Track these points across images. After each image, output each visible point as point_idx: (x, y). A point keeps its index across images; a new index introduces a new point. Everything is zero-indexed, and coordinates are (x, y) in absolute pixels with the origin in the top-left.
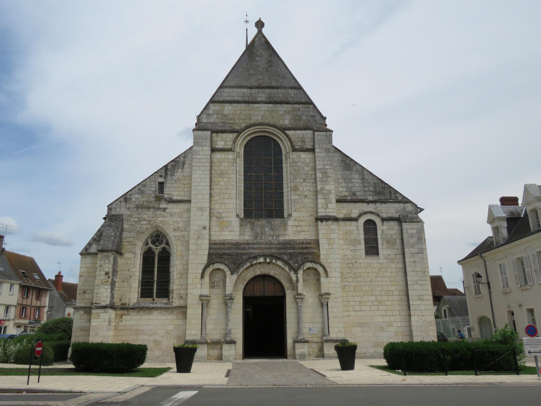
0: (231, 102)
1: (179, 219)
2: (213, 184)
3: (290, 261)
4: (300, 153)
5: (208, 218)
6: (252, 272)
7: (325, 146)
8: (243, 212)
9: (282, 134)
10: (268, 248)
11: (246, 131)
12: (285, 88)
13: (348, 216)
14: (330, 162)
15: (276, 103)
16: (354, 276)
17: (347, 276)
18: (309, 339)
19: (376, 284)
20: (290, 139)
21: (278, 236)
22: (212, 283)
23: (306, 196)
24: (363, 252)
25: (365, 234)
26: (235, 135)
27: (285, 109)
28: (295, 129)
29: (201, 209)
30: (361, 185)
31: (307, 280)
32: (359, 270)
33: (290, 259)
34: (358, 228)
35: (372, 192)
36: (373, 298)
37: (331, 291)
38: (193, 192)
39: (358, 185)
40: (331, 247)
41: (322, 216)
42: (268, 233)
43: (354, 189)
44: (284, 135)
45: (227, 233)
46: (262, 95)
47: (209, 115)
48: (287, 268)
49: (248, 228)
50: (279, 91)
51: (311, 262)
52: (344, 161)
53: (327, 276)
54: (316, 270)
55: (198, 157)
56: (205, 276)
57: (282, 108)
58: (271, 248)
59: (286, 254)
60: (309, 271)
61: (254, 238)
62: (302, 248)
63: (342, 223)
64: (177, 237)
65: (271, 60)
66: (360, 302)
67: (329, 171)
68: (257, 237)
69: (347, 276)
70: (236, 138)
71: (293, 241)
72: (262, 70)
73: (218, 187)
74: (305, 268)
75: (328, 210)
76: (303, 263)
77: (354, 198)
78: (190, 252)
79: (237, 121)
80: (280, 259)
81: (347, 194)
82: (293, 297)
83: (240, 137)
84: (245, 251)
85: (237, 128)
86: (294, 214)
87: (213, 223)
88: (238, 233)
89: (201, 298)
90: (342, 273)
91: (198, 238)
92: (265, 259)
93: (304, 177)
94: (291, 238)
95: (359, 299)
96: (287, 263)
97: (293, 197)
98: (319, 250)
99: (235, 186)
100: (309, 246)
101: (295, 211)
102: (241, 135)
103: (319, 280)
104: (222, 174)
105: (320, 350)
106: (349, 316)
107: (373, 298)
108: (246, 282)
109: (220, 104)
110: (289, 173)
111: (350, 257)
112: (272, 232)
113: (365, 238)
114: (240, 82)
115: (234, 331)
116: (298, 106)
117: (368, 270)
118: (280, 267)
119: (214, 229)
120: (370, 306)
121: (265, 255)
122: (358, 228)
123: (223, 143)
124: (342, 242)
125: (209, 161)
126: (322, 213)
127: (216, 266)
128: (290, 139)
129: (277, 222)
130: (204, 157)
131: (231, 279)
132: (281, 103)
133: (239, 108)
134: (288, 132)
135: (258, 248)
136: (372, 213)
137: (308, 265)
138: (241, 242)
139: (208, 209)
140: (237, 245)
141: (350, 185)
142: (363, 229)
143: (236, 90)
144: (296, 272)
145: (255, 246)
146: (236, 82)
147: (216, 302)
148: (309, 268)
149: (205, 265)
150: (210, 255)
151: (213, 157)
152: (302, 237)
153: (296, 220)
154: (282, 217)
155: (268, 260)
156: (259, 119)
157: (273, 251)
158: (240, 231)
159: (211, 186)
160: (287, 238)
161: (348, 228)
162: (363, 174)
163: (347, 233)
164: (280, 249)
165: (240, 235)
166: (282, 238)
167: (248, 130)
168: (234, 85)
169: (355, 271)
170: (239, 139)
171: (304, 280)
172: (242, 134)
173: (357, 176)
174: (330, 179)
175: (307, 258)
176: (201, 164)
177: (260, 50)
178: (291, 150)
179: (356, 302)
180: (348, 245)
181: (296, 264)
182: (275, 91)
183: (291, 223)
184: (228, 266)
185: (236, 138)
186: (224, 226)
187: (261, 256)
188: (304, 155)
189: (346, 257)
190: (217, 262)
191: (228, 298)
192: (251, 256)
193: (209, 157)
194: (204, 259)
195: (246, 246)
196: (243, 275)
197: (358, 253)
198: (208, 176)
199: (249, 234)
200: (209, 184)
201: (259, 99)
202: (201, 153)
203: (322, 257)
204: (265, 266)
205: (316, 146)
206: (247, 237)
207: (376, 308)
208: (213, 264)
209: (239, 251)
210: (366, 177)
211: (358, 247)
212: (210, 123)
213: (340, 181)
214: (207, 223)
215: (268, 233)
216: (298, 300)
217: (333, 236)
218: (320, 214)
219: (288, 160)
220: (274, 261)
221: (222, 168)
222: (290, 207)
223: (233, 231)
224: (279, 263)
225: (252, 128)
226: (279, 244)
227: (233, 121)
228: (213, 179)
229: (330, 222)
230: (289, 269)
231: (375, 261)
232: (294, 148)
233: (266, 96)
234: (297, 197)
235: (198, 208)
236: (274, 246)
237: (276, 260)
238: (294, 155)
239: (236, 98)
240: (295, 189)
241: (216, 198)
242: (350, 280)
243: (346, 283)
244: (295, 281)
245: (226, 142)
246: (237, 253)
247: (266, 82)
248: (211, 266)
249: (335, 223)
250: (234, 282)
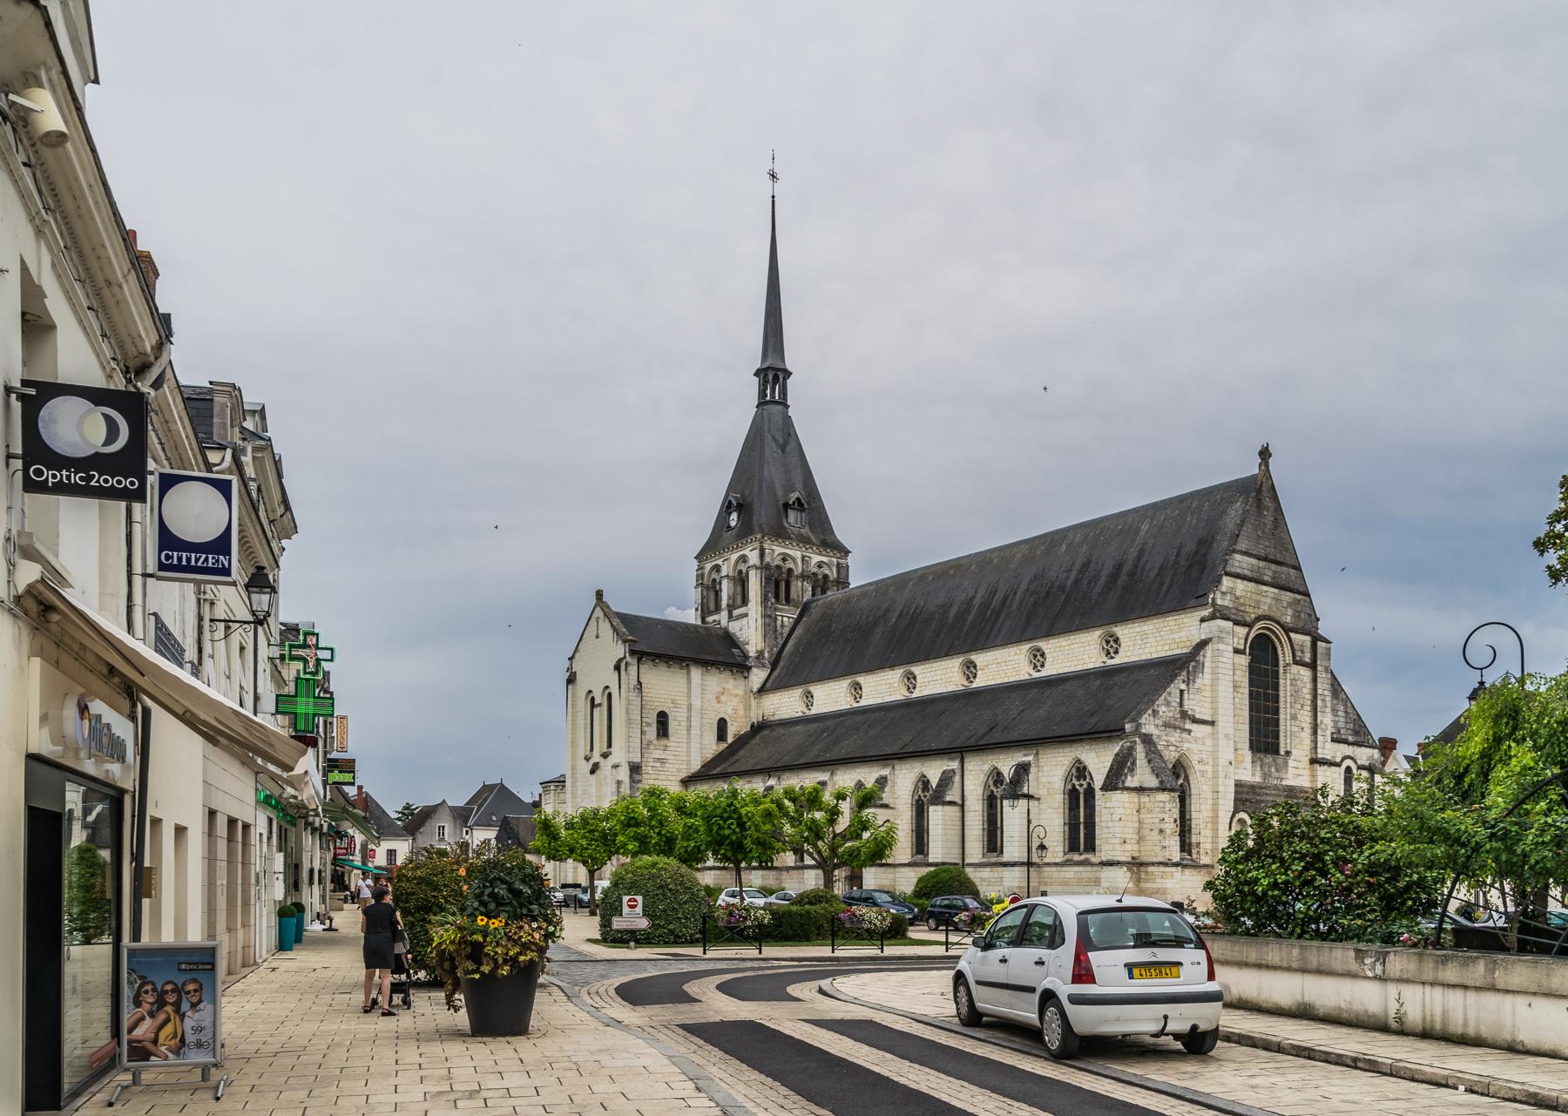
38: (1221, 711)
86: (1294, 752)
154: (1277, 753)
183: (1291, 763)
238: (1295, 669)
240: (1294, 717)
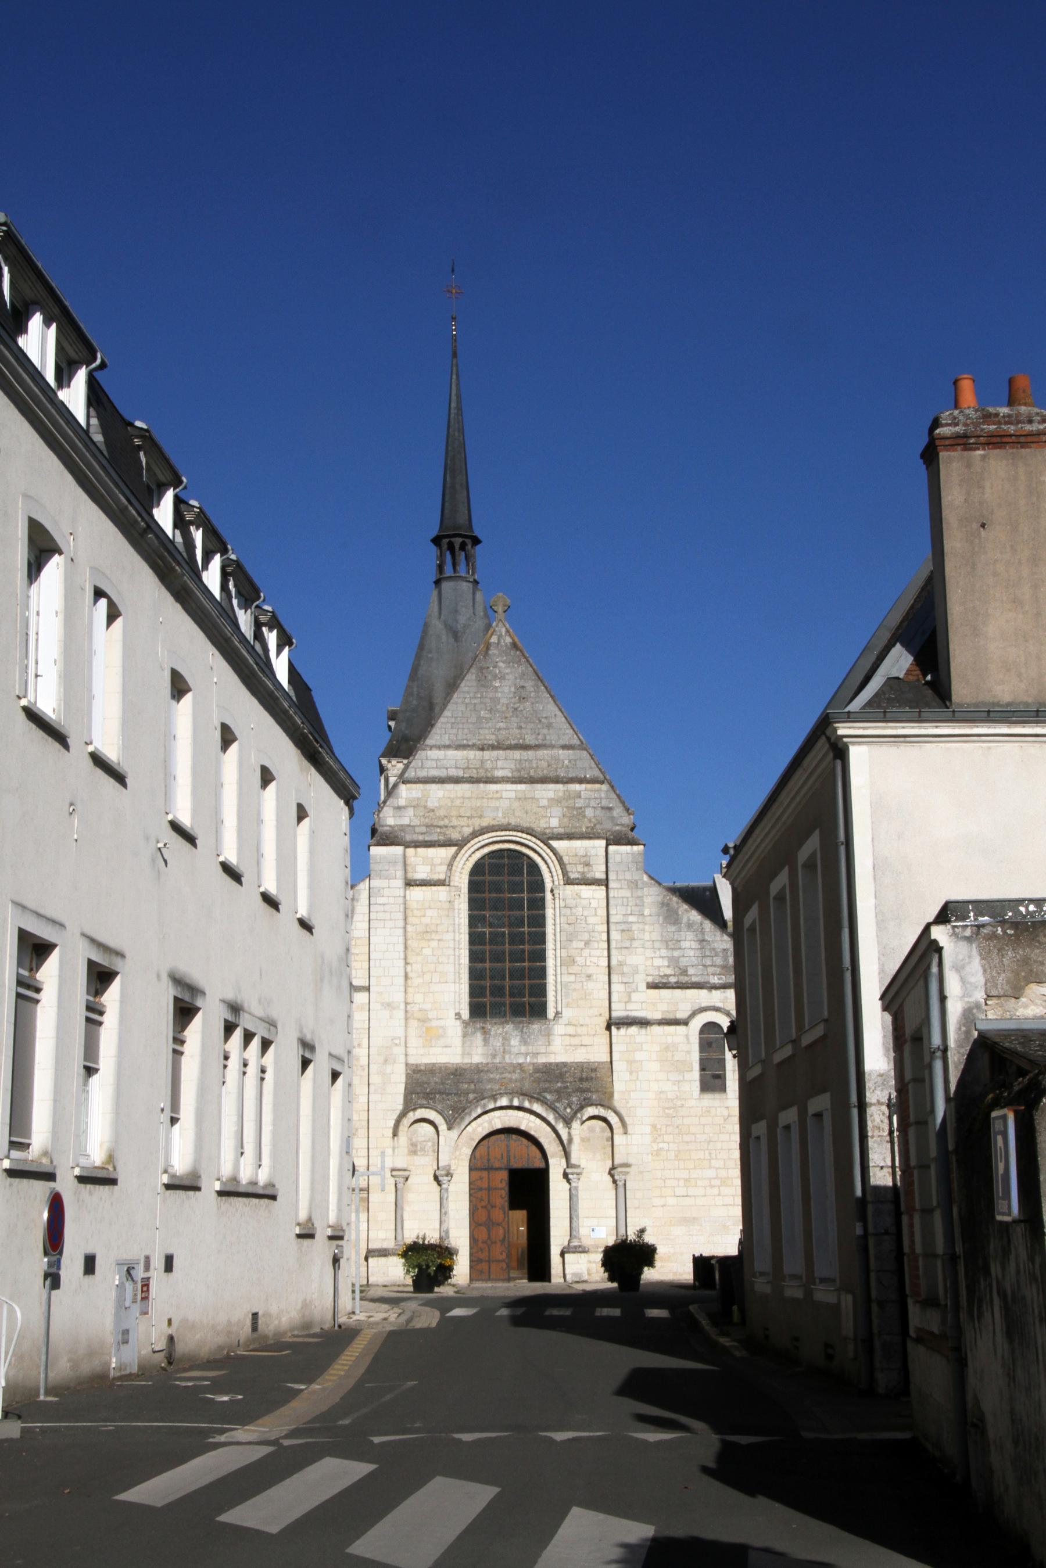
0: (442, 781)
2: (409, 953)
3: (557, 1105)
4: (580, 887)
5: (403, 1022)
7: (628, 876)
8: (467, 1007)
9: (545, 848)
11: (472, 842)
12: (553, 747)
13: (671, 1016)
14: (637, 909)
15: (532, 781)
16: (677, 1131)
17: (663, 1132)
19: (719, 1145)
20: (560, 860)
23: (589, 976)
24: (696, 1085)
26: (453, 850)
27: (551, 795)
28: (570, 837)
29: (389, 1006)
30: (698, 953)
32: (686, 1121)
33: (559, 1100)
34: (688, 1039)
35: (718, 966)
36: (711, 1173)
37: (631, 1161)
39: (692, 953)
41: (619, 1018)
42: (515, 1050)
43: (684, 962)
44: (548, 851)
46: (504, 763)
47: (399, 808)
49: (479, 1037)
50: (542, 753)
51: (596, 1105)
52: (668, 905)
55: (380, 900)
57: (547, 792)
59: (550, 1092)
65: (523, 687)
66: (686, 1180)
67: (635, 927)
69: (663, 1132)
70: (455, 857)
71: (565, 1064)
72: (504, 708)
73: (419, 959)
75: (630, 1006)
76: (582, 1108)
77: (684, 979)
79: (455, 822)
80: (538, 1100)
81: (669, 971)
83: (460, 855)
84: (472, 1086)
85: (455, 836)
86: (567, 1013)
87: (412, 1032)
88: (459, 1050)
89: (394, 1173)
90: (654, 1126)
91: (386, 1061)
92: (511, 1101)
93: (586, 936)
95: (684, 1174)
96: (551, 1107)
97: (566, 979)
99: (452, 957)
101: (568, 1005)
102: (463, 851)
104: (426, 933)
107: (711, 1173)
109: (421, 786)
110: (558, 930)
111: (670, 1095)
112: (523, 1049)
113: (701, 1060)
114: (459, 737)
115: (452, 1234)
116: (577, 787)
117: (703, 1120)
119: (413, 1042)
120: (705, 1187)
122: (688, 1039)
123: (428, 868)
125: (402, 909)
127: (421, 1113)
128: (560, 860)
129: (536, 1026)
130: (392, 900)
132: (544, 780)
133: (460, 794)
134: (555, 844)
136: (717, 1009)
137: (591, 1111)
139: (402, 1006)
140: (458, 1073)
141: (676, 954)
142: (697, 1041)
143: (451, 753)
144: (568, 1122)
146: (453, 737)
147: (422, 1182)
149: (398, 1113)
151: (408, 898)
153: (569, 1024)
156: (501, 819)
158: (463, 1046)
159: (405, 959)
160: (552, 1059)
161: (670, 1040)
162: (703, 932)
165: (463, 1054)
166: (542, 1060)
167: (476, 840)
168: (447, 743)
169: (679, 1122)
170: (458, 859)
171: (583, 1140)
172: (465, 848)
173: (690, 935)
174: (636, 944)
175: (588, 1099)
176: (387, 916)
177: (501, 664)
178: (562, 882)
179: (678, 1179)
181: (568, 1110)
182: (530, 753)
183: (559, 1029)
185: (455, 857)
186: (431, 1035)
188: (586, 891)
189: (663, 1096)
190: (422, 1107)
193: (401, 900)
194: (398, 1103)
197: (686, 1087)
198: (401, 939)
200: (402, 955)
201: (499, 773)
202: (386, 892)
203: (616, 1096)
205: (611, 876)
206: (477, 1055)
207: (715, 1191)
208: (414, 1110)
210: (707, 938)
211: (688, 1076)
212: (403, 828)
213: (657, 945)
214: (400, 1032)
215: (515, 1050)
217: (639, 1056)
218: (614, 1014)
219: (557, 901)
221: (426, 920)
222: (559, 998)
224: (537, 1107)
225: (485, 836)
227: (446, 822)
228: (409, 942)
230: (556, 1118)
231: (717, 1103)
232: (568, 878)
233: (513, 766)
234: (572, 978)
237: (530, 1102)
239: (453, 772)
240: (569, 961)
241: (415, 981)
243: (661, 1145)
245: (433, 865)
247: (513, 736)
248: (411, 1114)
249: (643, 1031)
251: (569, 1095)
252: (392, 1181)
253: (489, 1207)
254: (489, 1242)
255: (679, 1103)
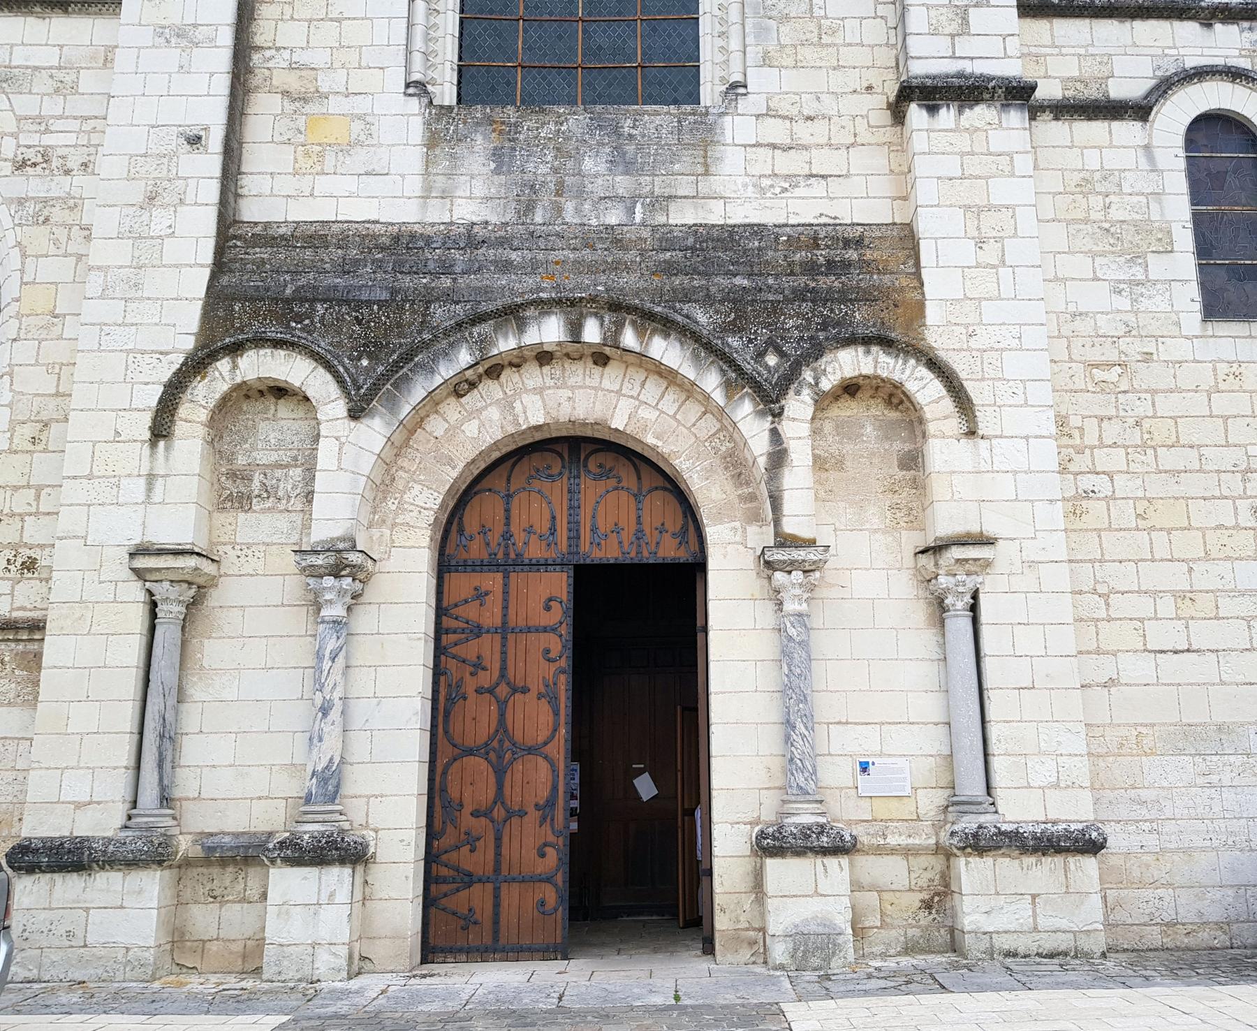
1: (52, 107)
3: (734, 341)
6: (494, 413)
10: (593, 269)
16: (1136, 437)
17: (1091, 438)
18: (858, 831)
21: (661, 202)
22: (233, 475)
24: (1189, 296)
25: (1196, 196)
29: (182, 35)
31: (840, 464)
33: (735, 328)
34: (1151, 158)
40: (990, 254)
42: (598, 187)
45: (347, 184)
48: (711, 382)
49: (476, 156)
51: (867, 341)
53: (971, 433)
54: (895, 396)
56: (180, 428)
58: (616, 267)
59: (708, 300)
60: (848, 409)
61: (510, 216)
62: (811, 268)
63: (1054, 130)
64: (31, 208)
68: (530, 208)
74: (826, 385)
75: (965, 46)
76: (816, 351)
78: (95, 283)
80: (667, 326)
82: (749, 561)
84: (446, 282)
88: (414, 185)
89: (141, 563)
90: (1062, 421)
92: (575, 329)
94: (739, 215)
96: (709, 347)
98: (918, 275)
100: (852, 255)
103: (913, 461)
105: (928, 905)
106: (1110, 683)
108: (450, 475)
112: (623, 183)
115: (357, 782)
117: (1221, 404)
118: (668, 375)
121: (573, 303)
122: (1151, 158)
124: (1057, 236)
126: (931, 59)
127: (259, 365)
131: (348, 447)
135: (534, 267)
137: (847, 363)
138: (429, 231)
140: (402, 247)
142: (1182, 164)
144: (770, 400)
145: (514, 256)
148: (850, 389)
150: (218, 299)
152: (804, 208)
155: (592, 332)
157: (628, 281)
158: (427, 173)
160: (715, 215)
161: (1092, 160)
163: (1085, 186)
164: (669, 269)
166: (683, 216)
169: (1143, 408)
171: (819, 463)
175: (838, 324)
180: (1094, 255)
181: (772, 360)
184: (329, 367)
187: (545, 307)
190: (260, 341)
191: (319, 560)
192: (484, 307)
194: (183, 328)
195: (456, 254)
196: (436, 426)
197: (1156, 302)
199: (480, 189)
203: (933, 314)
204: (581, 375)
208: (236, 349)
209: (406, 281)
211: (1158, 266)
216: (779, 576)
217: (1002, 191)
220: (629, 338)
223: (374, 158)
224: (665, 350)
226: (667, 239)
229: (981, 114)
230: (728, 386)
235: (160, 30)
236: (632, 255)
237: (640, 333)
242: (1113, 460)
243: (1087, 482)
244: (762, 462)
246: (394, 292)
248: (223, 365)
250: (367, 463)
251: (775, 309)
252: (135, 592)
253: (503, 690)
254: (499, 813)
255: (1133, 348)
